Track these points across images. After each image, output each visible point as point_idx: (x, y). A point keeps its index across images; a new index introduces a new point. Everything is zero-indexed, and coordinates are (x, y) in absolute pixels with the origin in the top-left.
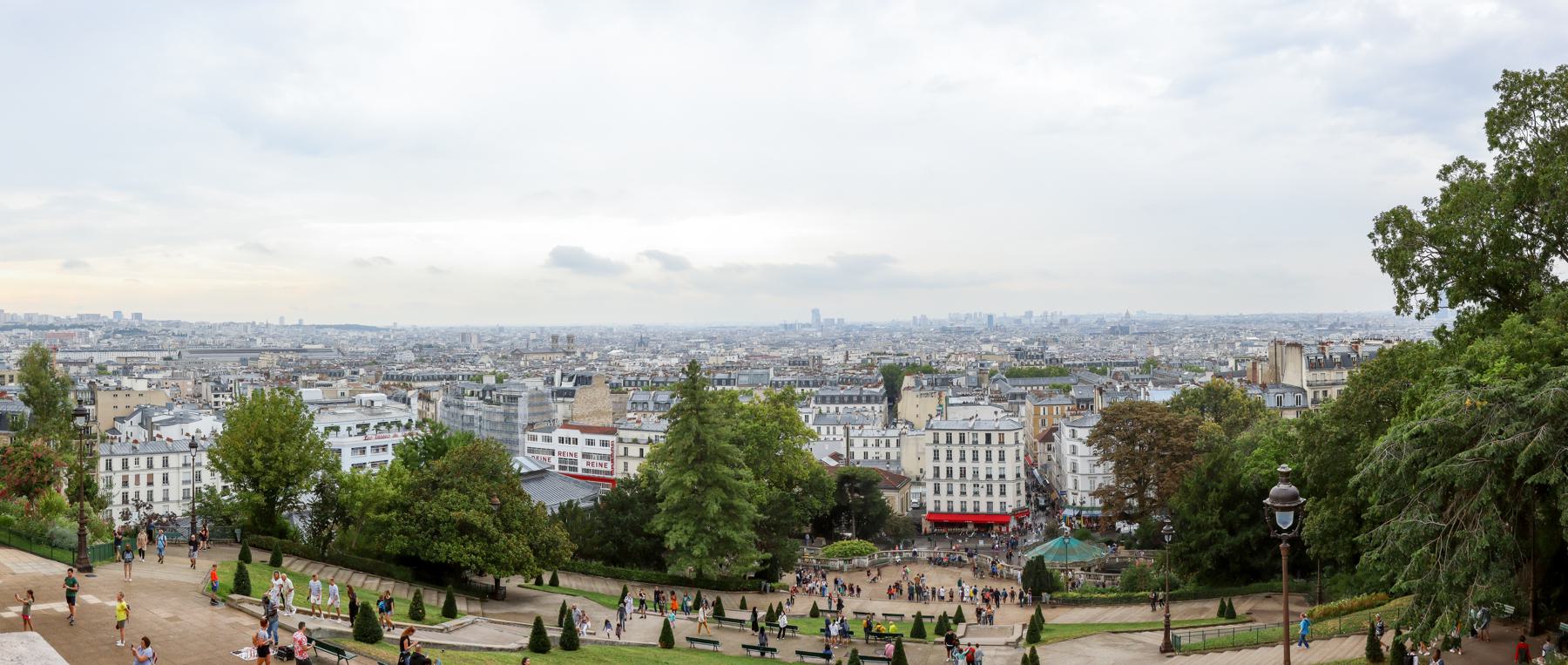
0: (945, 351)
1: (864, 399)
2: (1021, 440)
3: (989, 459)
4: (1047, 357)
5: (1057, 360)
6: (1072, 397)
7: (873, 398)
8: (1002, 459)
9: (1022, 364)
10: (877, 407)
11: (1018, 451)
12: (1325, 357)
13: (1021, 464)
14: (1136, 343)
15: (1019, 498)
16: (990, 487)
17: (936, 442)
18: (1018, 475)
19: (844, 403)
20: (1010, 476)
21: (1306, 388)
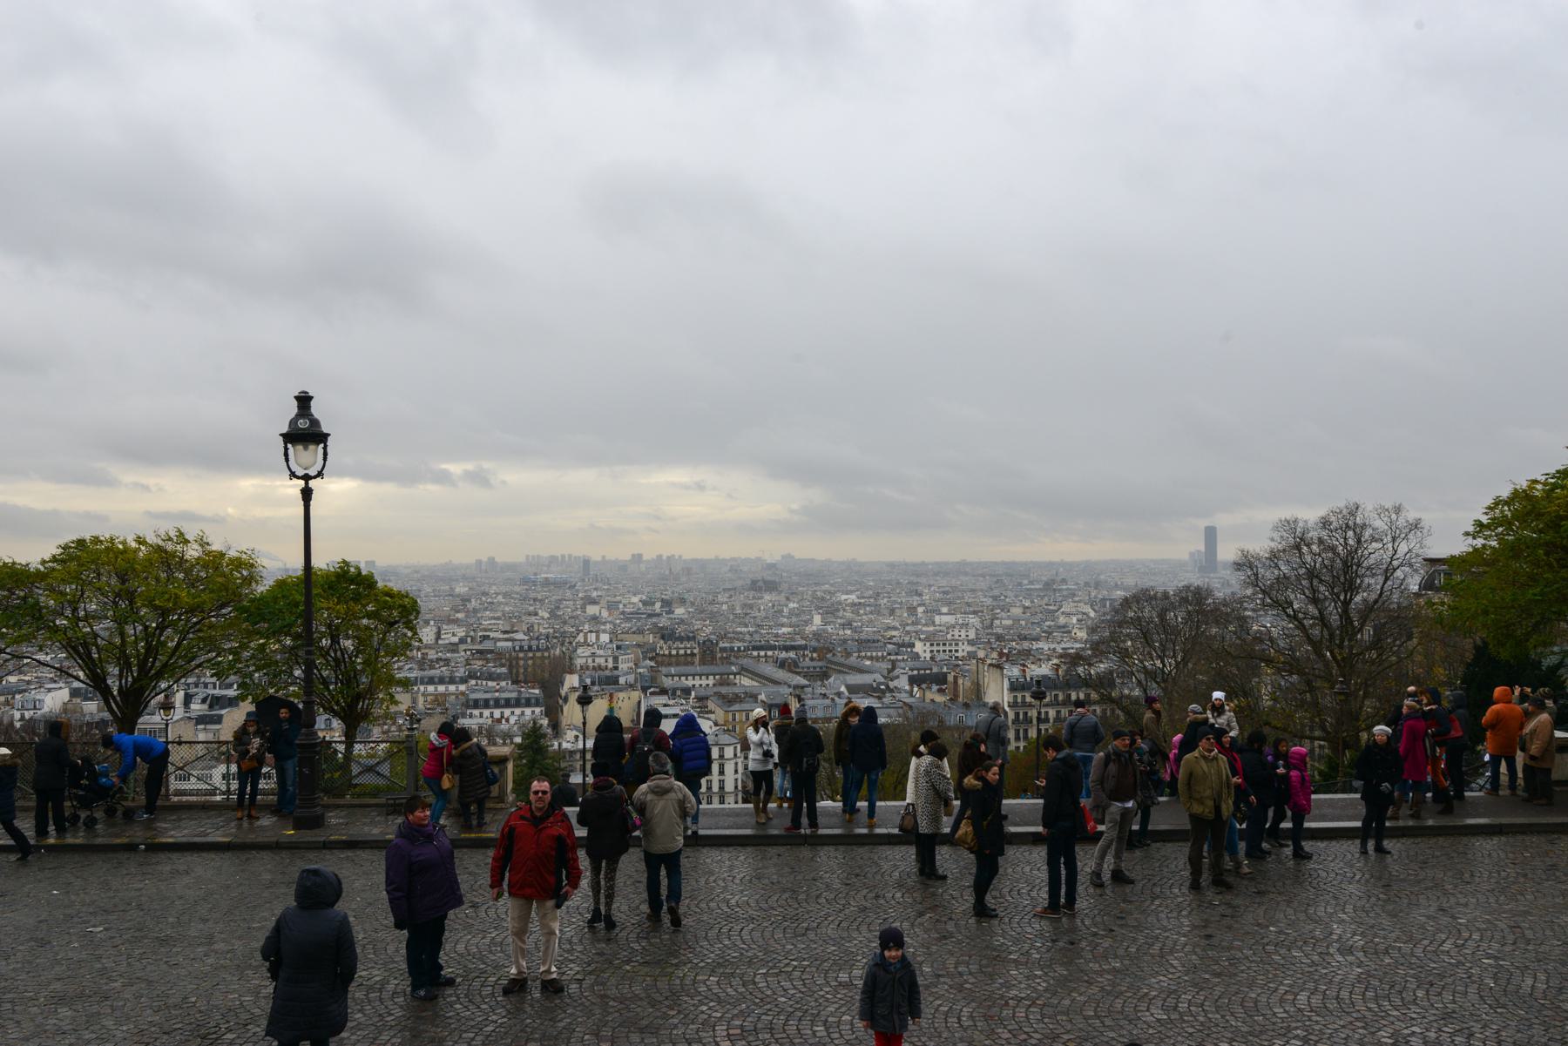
0: (536, 614)
1: (523, 701)
2: (739, 755)
5: (712, 642)
6: (762, 701)
7: (533, 701)
8: (722, 772)
9: (670, 648)
10: (538, 710)
11: (736, 764)
13: (739, 776)
18: (736, 787)
19: (503, 707)
20: (729, 787)
21: (1007, 708)
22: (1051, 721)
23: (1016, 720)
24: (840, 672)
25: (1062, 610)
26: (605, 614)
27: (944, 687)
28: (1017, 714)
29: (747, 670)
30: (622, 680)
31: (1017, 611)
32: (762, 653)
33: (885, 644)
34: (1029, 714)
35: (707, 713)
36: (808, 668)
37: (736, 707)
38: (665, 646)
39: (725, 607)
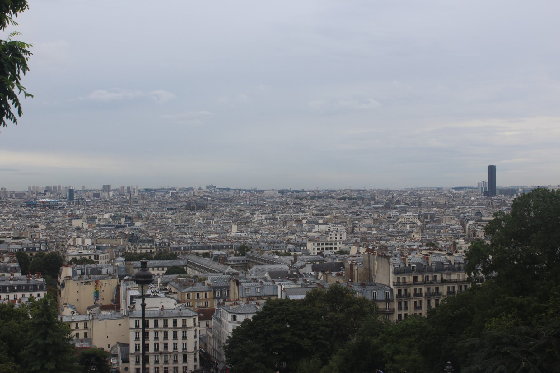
2: (197, 324)
3: (175, 337)
4: (157, 241)
6: (208, 285)
8: (184, 337)
9: (135, 248)
11: (195, 331)
12: (405, 265)
13: (197, 340)
14: (213, 220)
15: (196, 363)
16: (176, 357)
17: (137, 326)
18: (195, 348)
19: (14, 291)
20: (190, 348)
22: (424, 295)
23: (399, 296)
24: (257, 264)
25: (399, 221)
26: (86, 226)
27: (340, 272)
28: (400, 291)
29: (192, 264)
30: (104, 271)
31: (370, 222)
32: (201, 251)
33: (287, 244)
34: (408, 291)
35: (171, 293)
36: (234, 261)
37: (189, 289)
38: (132, 247)
39: (170, 221)
